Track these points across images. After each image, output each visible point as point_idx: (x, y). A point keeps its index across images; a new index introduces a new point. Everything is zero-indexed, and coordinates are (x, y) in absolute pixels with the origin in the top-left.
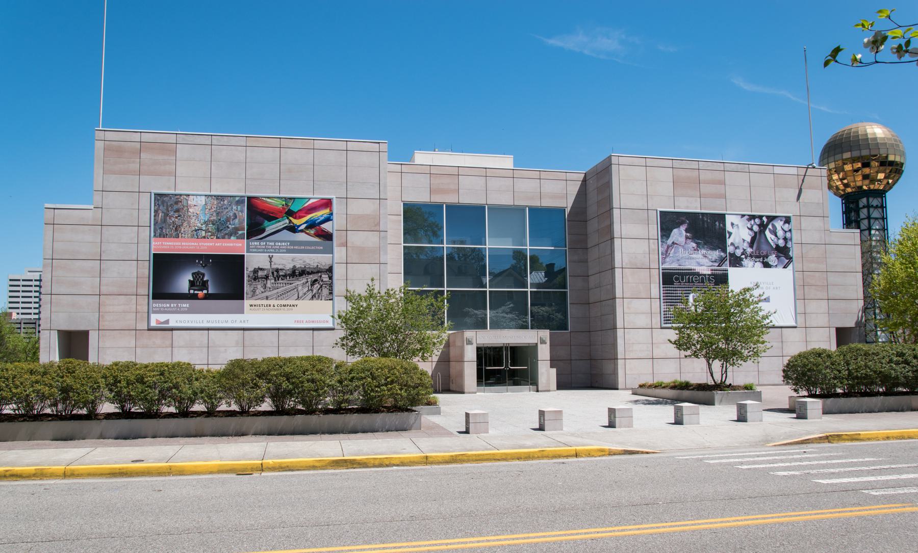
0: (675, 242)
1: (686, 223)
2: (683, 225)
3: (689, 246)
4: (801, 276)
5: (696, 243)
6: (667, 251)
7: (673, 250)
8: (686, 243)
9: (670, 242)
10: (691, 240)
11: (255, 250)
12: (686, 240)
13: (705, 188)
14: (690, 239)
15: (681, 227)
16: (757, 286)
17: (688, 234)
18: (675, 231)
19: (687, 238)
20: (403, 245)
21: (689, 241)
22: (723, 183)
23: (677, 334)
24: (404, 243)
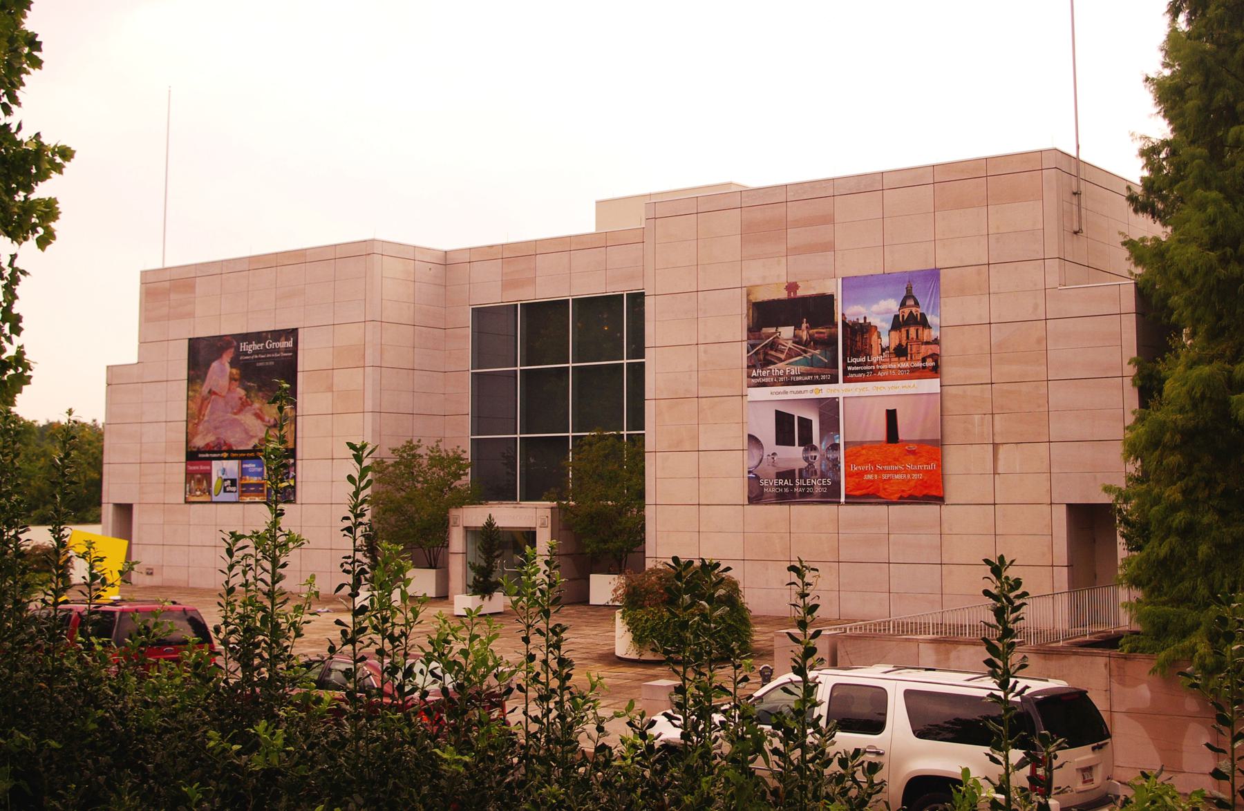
0: (214, 389)
1: (231, 347)
2: (229, 351)
3: (233, 395)
4: (987, 395)
5: (245, 389)
6: (200, 410)
7: (209, 406)
8: (229, 389)
9: (205, 390)
10: (237, 383)
11: (188, 489)
12: (230, 383)
13: (796, 236)
14: (236, 380)
15: (224, 356)
16: (458, 447)
17: (234, 371)
18: (215, 365)
19: (232, 379)
20: (471, 437)
21: (236, 384)
22: (829, 220)
23: (137, 563)
24: (472, 435)
